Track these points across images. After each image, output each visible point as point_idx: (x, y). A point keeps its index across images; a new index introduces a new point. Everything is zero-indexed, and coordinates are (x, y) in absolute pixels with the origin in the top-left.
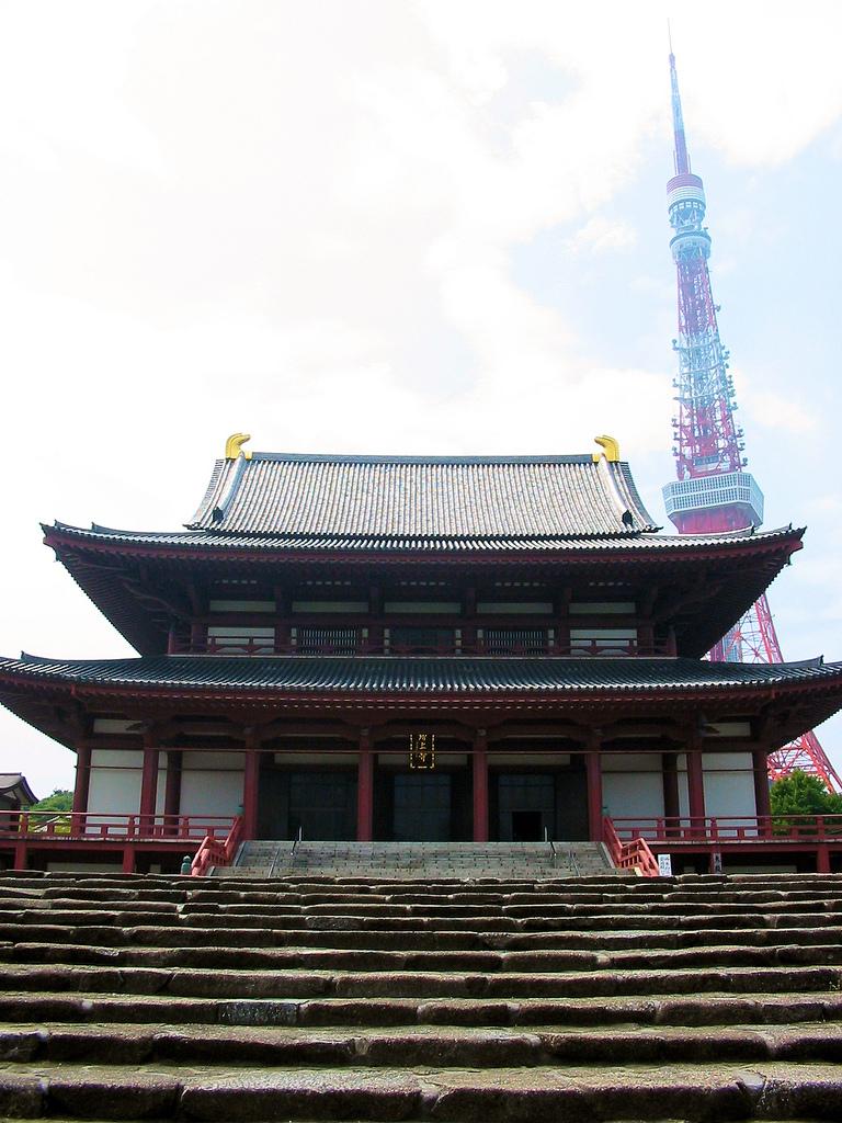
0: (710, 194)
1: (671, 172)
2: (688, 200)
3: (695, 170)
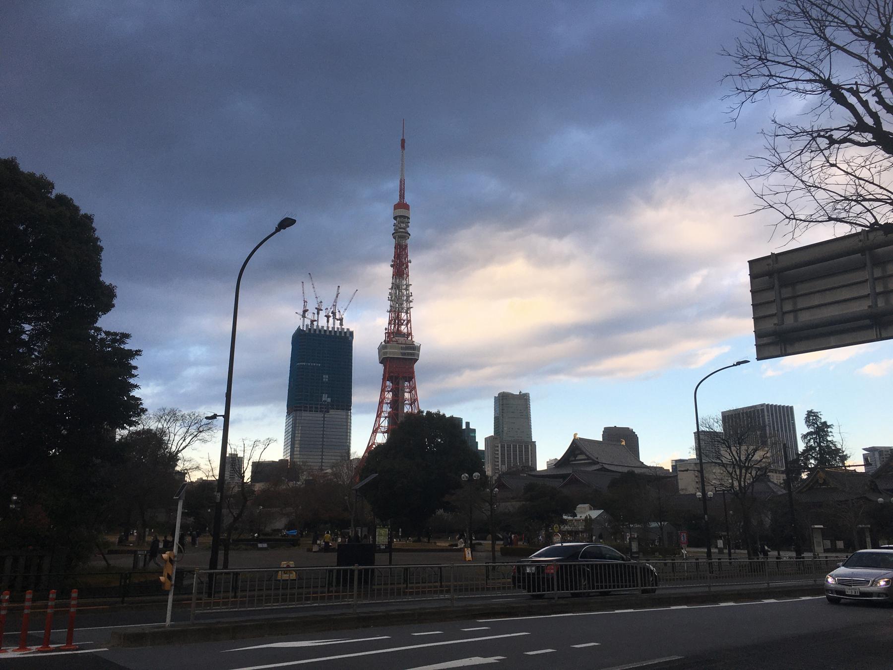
1: (396, 200)
3: (408, 199)
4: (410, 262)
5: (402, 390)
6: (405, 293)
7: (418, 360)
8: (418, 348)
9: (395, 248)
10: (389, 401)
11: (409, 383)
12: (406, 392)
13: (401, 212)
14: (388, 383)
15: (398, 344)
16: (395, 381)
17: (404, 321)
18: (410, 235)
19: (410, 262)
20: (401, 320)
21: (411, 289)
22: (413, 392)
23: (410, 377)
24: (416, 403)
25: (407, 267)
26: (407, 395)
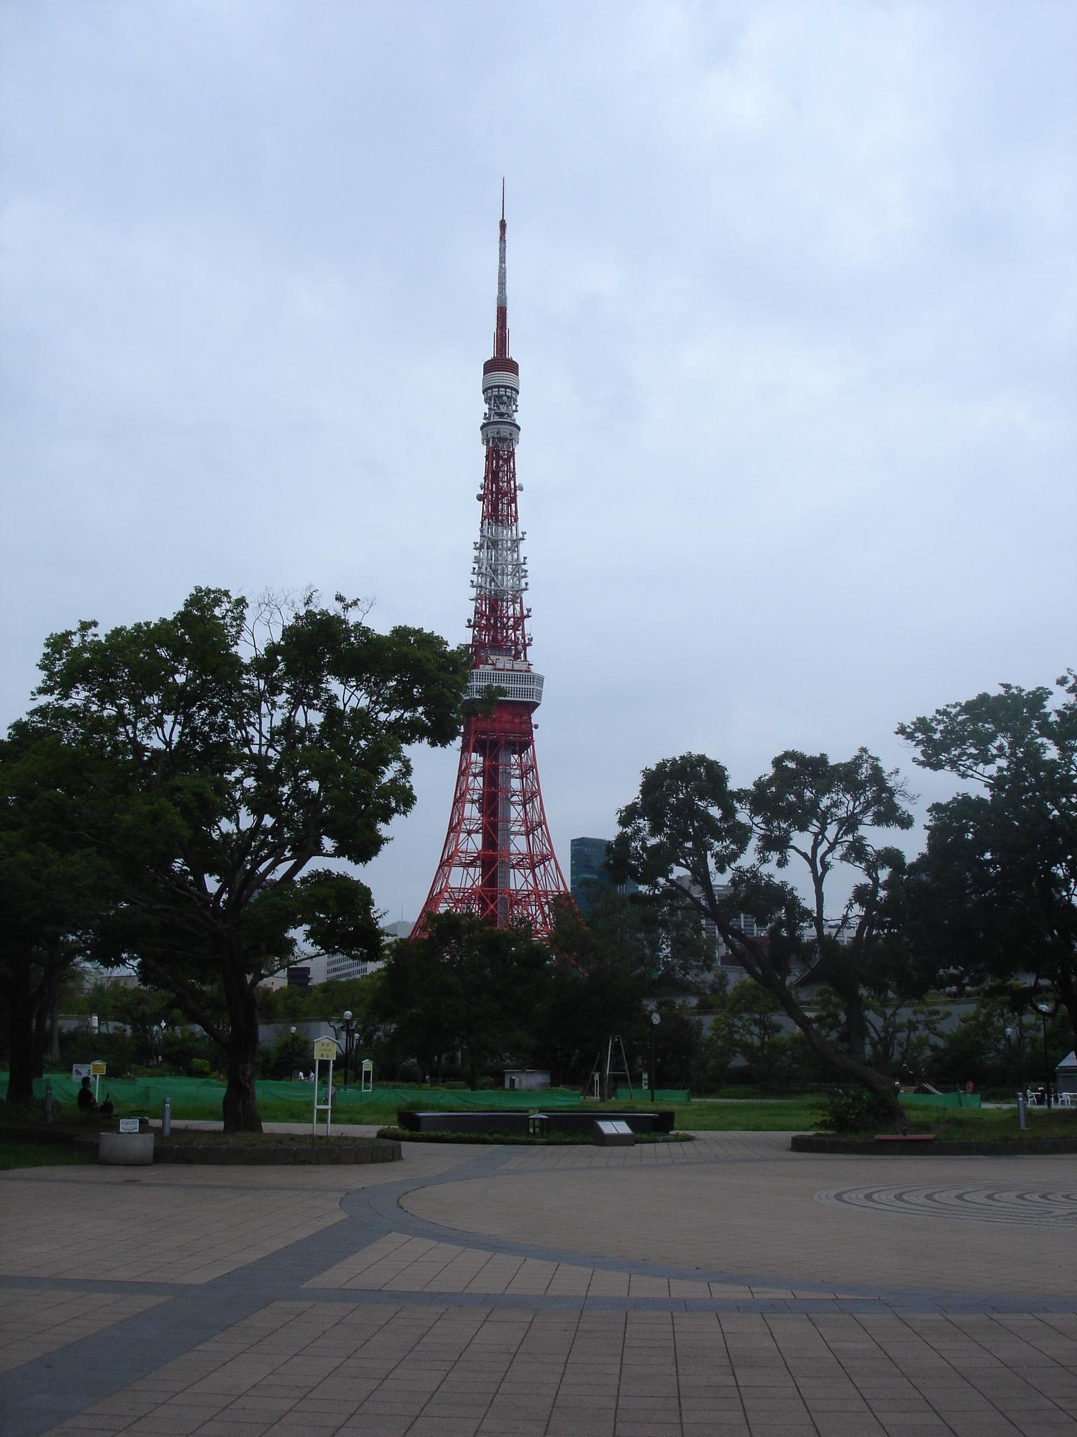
0: (525, 381)
1: (489, 354)
2: (502, 386)
3: (513, 353)
4: (521, 489)
5: (505, 772)
6: (509, 558)
7: (537, 705)
8: (540, 680)
9: (487, 457)
10: (475, 797)
11: (520, 756)
12: (513, 777)
13: (502, 377)
14: (475, 757)
15: (495, 669)
16: (491, 753)
17: (508, 619)
18: (519, 428)
19: (521, 489)
20: (502, 618)
21: (524, 548)
22: (530, 775)
23: (523, 742)
24: (537, 802)
25: (514, 500)
26: (516, 784)
